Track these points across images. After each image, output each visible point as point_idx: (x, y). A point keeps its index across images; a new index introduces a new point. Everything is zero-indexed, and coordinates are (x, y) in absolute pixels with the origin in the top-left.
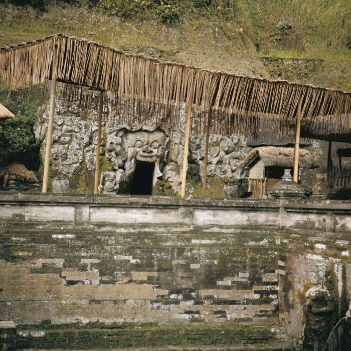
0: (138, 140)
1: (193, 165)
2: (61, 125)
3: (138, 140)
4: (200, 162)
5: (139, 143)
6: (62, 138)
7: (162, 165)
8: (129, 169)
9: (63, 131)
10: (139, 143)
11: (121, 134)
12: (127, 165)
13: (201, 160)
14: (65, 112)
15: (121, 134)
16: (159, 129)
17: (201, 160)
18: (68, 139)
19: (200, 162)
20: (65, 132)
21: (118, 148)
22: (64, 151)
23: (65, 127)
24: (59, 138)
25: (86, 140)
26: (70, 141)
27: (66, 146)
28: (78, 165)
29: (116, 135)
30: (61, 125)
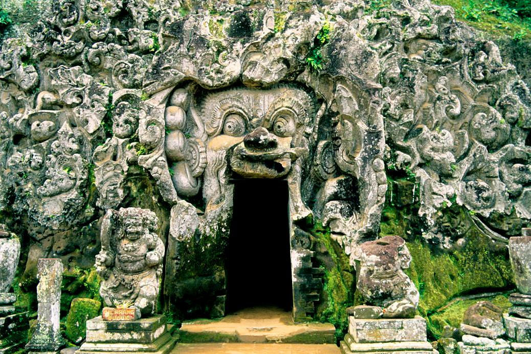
0: (230, 114)
1: (402, 182)
2: (32, 91)
3: (230, 114)
4: (420, 173)
5: (234, 121)
6: (34, 125)
7: (309, 185)
8: (214, 199)
9: (38, 107)
10: (234, 121)
11: (180, 97)
12: (211, 189)
13: (420, 165)
14: (42, 57)
15: (180, 97)
16: (291, 80)
17: (420, 165)
18: (46, 125)
19: (420, 173)
20: (42, 108)
21: (176, 141)
22: (38, 158)
23: (45, 95)
24: (28, 124)
25: (94, 123)
26: (53, 134)
27: (44, 144)
28: (74, 194)
29: (169, 102)
30: (32, 91)
